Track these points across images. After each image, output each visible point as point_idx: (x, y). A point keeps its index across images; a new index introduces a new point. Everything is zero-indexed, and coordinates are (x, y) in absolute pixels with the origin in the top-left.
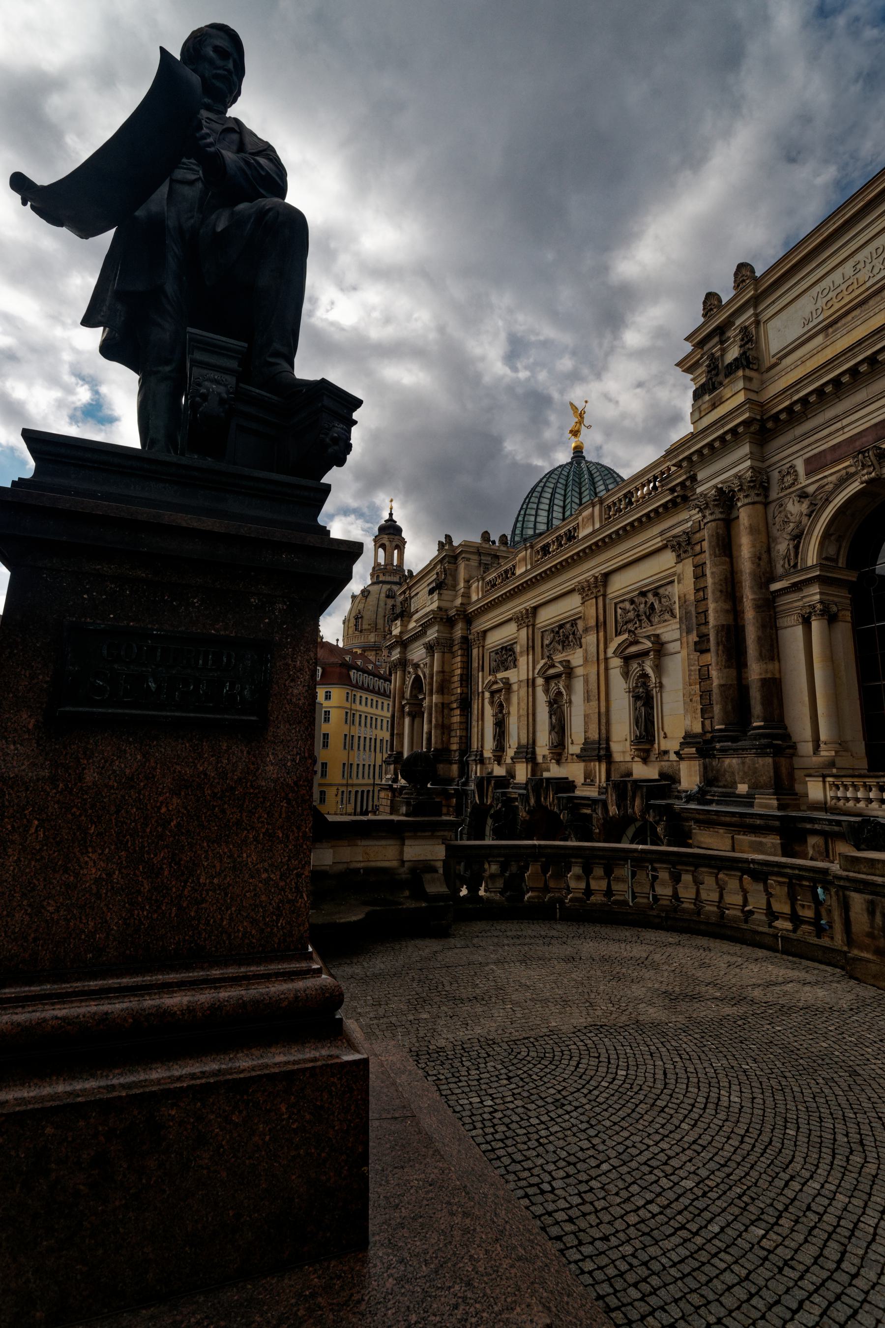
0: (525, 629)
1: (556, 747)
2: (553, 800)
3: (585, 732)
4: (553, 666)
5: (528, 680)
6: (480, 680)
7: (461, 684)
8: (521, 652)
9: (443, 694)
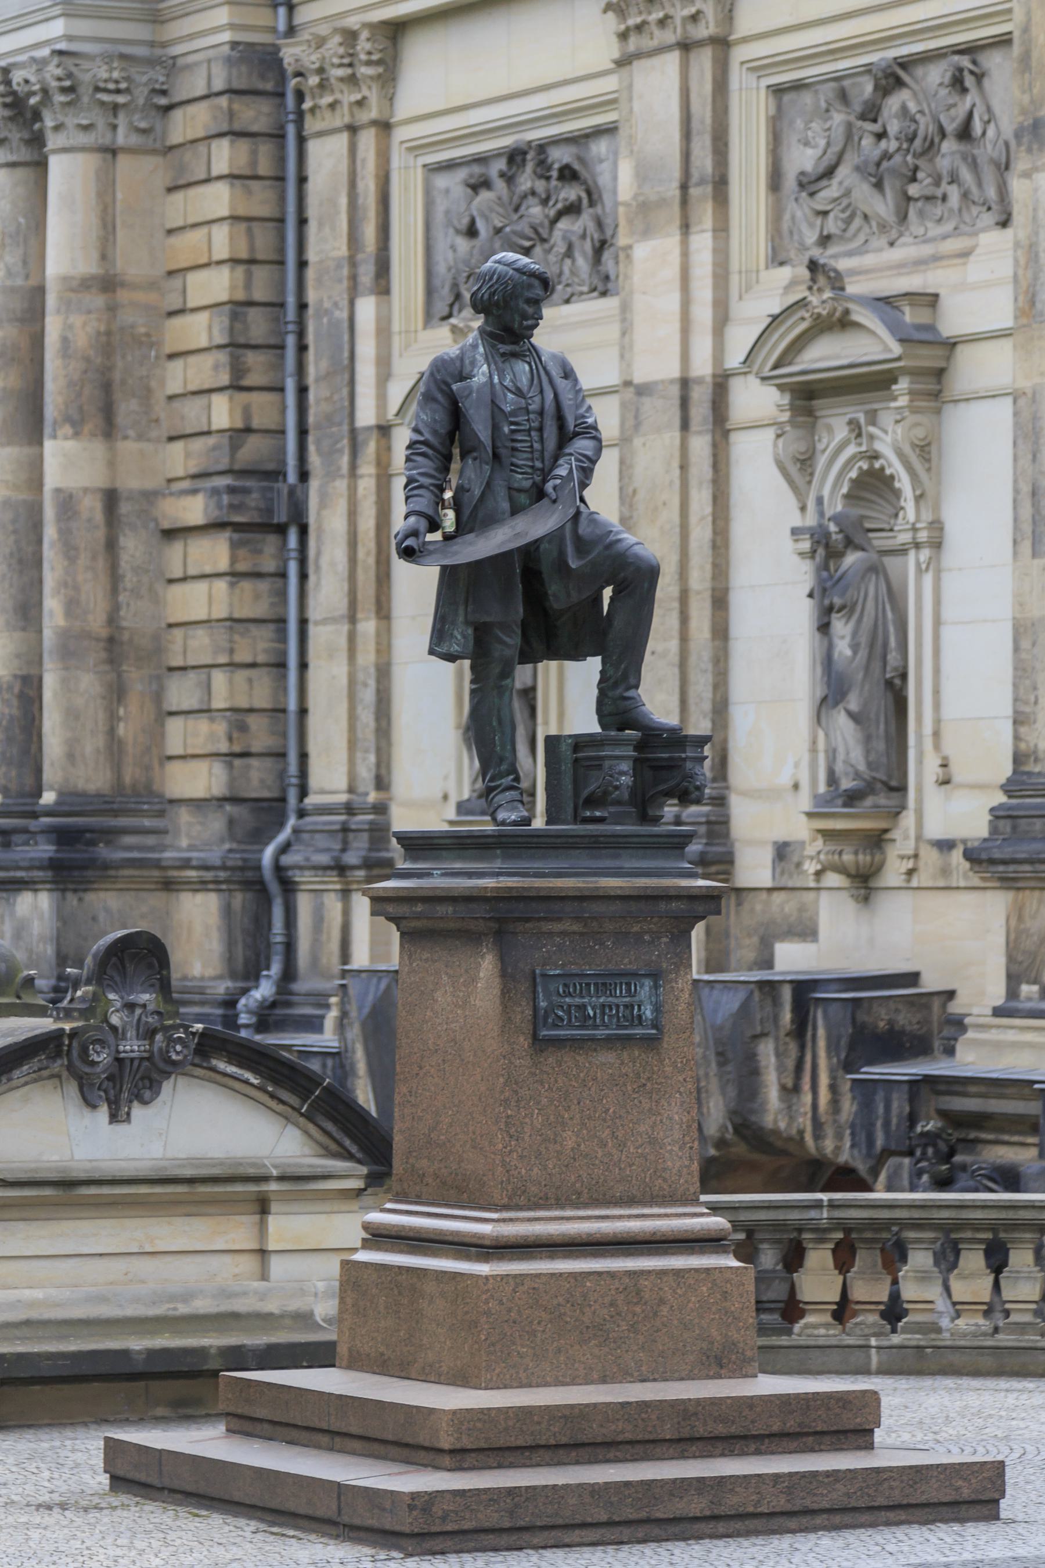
0: (673, 59)
1: (852, 798)
2: (835, 1102)
3: (1019, 720)
4: (844, 323)
5: (685, 383)
6: (366, 348)
7: (238, 370)
8: (644, 208)
9: (109, 429)
